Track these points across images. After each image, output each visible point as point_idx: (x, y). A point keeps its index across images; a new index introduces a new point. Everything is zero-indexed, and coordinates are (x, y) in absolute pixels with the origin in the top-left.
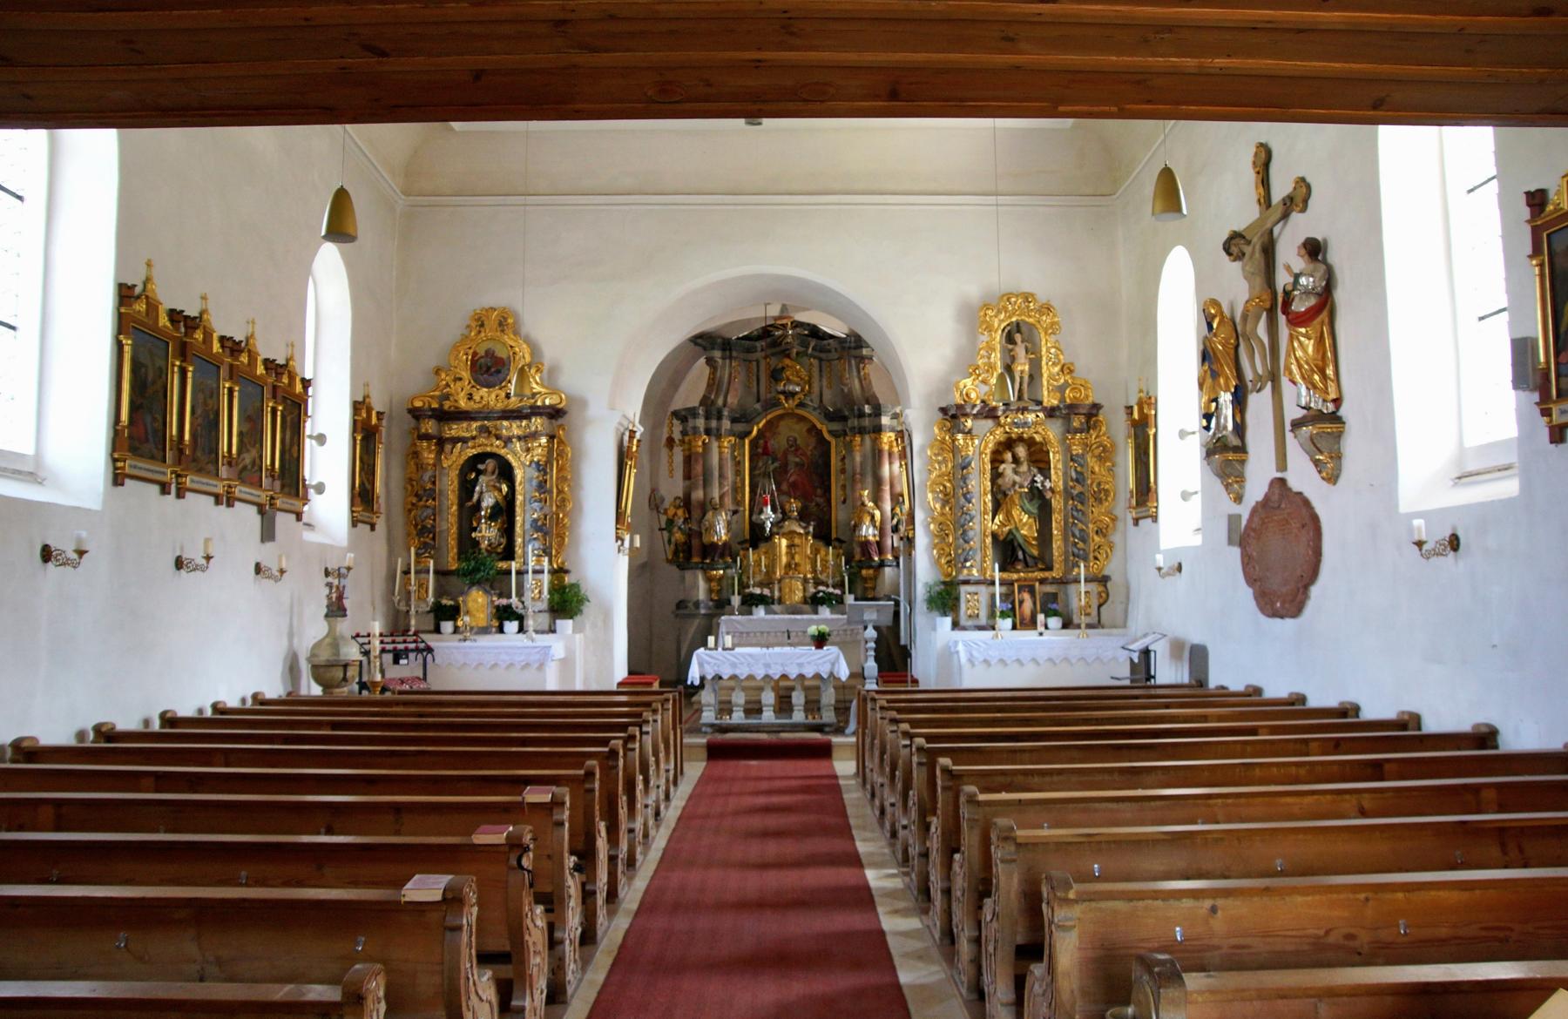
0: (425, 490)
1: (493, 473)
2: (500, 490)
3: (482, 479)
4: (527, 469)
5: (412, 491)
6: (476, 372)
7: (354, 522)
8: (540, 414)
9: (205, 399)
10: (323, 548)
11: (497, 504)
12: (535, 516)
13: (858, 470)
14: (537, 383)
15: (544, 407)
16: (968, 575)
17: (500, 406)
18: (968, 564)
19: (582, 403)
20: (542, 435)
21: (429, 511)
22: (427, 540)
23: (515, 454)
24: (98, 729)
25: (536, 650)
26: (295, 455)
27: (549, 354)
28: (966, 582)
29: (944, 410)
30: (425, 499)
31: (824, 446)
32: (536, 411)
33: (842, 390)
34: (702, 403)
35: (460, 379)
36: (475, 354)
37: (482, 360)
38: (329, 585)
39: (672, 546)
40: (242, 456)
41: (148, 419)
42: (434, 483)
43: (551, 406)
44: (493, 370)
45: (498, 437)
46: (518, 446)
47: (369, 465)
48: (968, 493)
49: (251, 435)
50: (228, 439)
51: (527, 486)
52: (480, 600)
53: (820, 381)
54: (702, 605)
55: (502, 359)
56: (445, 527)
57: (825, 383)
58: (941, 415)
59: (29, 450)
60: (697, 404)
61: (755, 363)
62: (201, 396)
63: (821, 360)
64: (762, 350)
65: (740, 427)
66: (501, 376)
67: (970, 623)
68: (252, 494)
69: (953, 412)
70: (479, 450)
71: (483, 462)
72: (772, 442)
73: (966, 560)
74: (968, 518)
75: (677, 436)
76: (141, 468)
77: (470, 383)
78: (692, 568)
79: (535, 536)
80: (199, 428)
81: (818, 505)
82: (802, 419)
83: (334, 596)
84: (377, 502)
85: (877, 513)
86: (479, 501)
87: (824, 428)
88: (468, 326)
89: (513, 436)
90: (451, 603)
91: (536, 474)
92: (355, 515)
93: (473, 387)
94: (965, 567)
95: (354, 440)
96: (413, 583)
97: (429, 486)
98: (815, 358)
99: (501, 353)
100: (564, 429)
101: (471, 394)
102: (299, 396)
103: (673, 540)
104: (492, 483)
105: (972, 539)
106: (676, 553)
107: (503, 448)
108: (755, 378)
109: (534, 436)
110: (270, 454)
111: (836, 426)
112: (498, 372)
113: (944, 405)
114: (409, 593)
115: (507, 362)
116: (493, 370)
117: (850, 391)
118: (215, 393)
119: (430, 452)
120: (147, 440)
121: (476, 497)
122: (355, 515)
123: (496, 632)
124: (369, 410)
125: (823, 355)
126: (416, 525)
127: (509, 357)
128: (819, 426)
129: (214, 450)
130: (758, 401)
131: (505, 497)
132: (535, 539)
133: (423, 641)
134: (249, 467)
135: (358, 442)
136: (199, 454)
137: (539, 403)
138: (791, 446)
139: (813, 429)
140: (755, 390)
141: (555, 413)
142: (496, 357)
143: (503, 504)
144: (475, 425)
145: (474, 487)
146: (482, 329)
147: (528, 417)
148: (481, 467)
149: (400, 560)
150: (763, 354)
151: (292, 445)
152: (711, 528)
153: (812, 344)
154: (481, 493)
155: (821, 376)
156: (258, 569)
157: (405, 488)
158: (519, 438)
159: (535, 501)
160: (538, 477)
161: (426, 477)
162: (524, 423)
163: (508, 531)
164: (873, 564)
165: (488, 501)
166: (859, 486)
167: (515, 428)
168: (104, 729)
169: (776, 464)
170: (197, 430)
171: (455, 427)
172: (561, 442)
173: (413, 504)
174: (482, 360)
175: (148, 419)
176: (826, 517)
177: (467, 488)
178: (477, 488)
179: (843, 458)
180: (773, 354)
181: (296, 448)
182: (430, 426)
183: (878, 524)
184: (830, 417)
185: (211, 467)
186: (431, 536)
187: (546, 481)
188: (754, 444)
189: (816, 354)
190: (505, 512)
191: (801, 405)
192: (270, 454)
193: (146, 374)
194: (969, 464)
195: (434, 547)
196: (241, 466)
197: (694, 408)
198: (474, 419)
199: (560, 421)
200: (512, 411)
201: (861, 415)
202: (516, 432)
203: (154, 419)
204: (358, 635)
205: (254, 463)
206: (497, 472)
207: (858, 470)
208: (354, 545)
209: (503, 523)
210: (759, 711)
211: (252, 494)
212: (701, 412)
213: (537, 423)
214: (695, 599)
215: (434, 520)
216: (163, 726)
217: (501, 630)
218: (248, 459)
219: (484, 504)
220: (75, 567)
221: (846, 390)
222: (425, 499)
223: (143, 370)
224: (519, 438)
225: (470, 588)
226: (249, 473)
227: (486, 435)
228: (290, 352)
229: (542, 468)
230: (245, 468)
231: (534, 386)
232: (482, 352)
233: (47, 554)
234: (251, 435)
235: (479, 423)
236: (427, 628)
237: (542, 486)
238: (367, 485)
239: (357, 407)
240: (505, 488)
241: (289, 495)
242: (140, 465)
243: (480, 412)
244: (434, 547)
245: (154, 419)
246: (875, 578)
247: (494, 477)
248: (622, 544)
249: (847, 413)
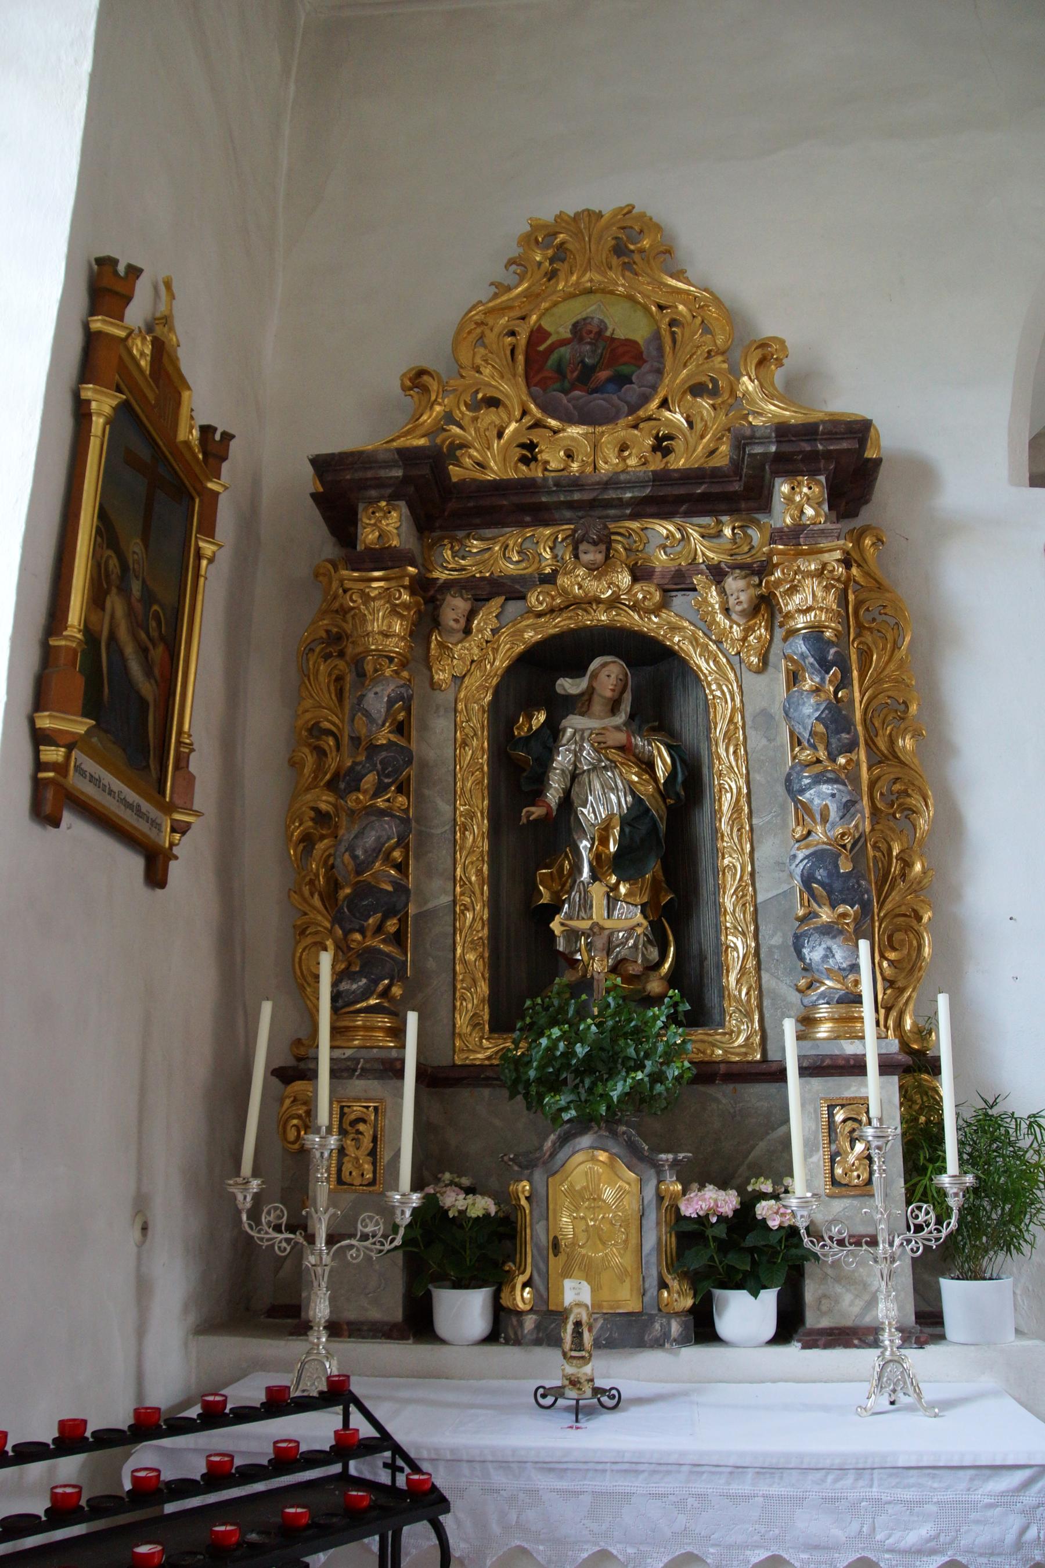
0: (373, 749)
1: (614, 707)
2: (648, 766)
3: (573, 724)
5: (319, 769)
6: (543, 384)
21: (390, 828)
22: (376, 942)
25: (1019, 1477)
30: (369, 780)
35: (493, 402)
37: (565, 351)
42: (401, 729)
44: (604, 375)
52: (608, 1194)
56: (445, 899)
66: (632, 391)
71: (578, 669)
77: (524, 413)
79: (826, 915)
84: (182, 763)
86: (567, 804)
88: (511, 262)
90: (482, 1206)
92: (53, 754)
93: (538, 425)
95: (81, 413)
96: (323, 1116)
97: (384, 736)
101: (531, 446)
104: (621, 738)
112: (622, 380)
114: (302, 1155)
116: (604, 375)
119: (394, 611)
121: (553, 796)
122: (53, 754)
123: (684, 1341)
126: (330, 896)
127: (657, 336)
135: (98, 423)
142: (612, 340)
143: (657, 810)
146: (563, 267)
149: (267, 1009)
154: (574, 776)
157: (295, 764)
161: (377, 701)
171: (476, 545)
173: (321, 818)
174: (565, 351)
186: (392, 925)
195: (398, 974)
202: (705, 551)
206: (626, 707)
209: (655, 889)
215: (401, 868)
222: (369, 780)
224: (717, 574)
225: (565, 1139)
232: (565, 333)
236: (375, 1314)
244: (398, 974)
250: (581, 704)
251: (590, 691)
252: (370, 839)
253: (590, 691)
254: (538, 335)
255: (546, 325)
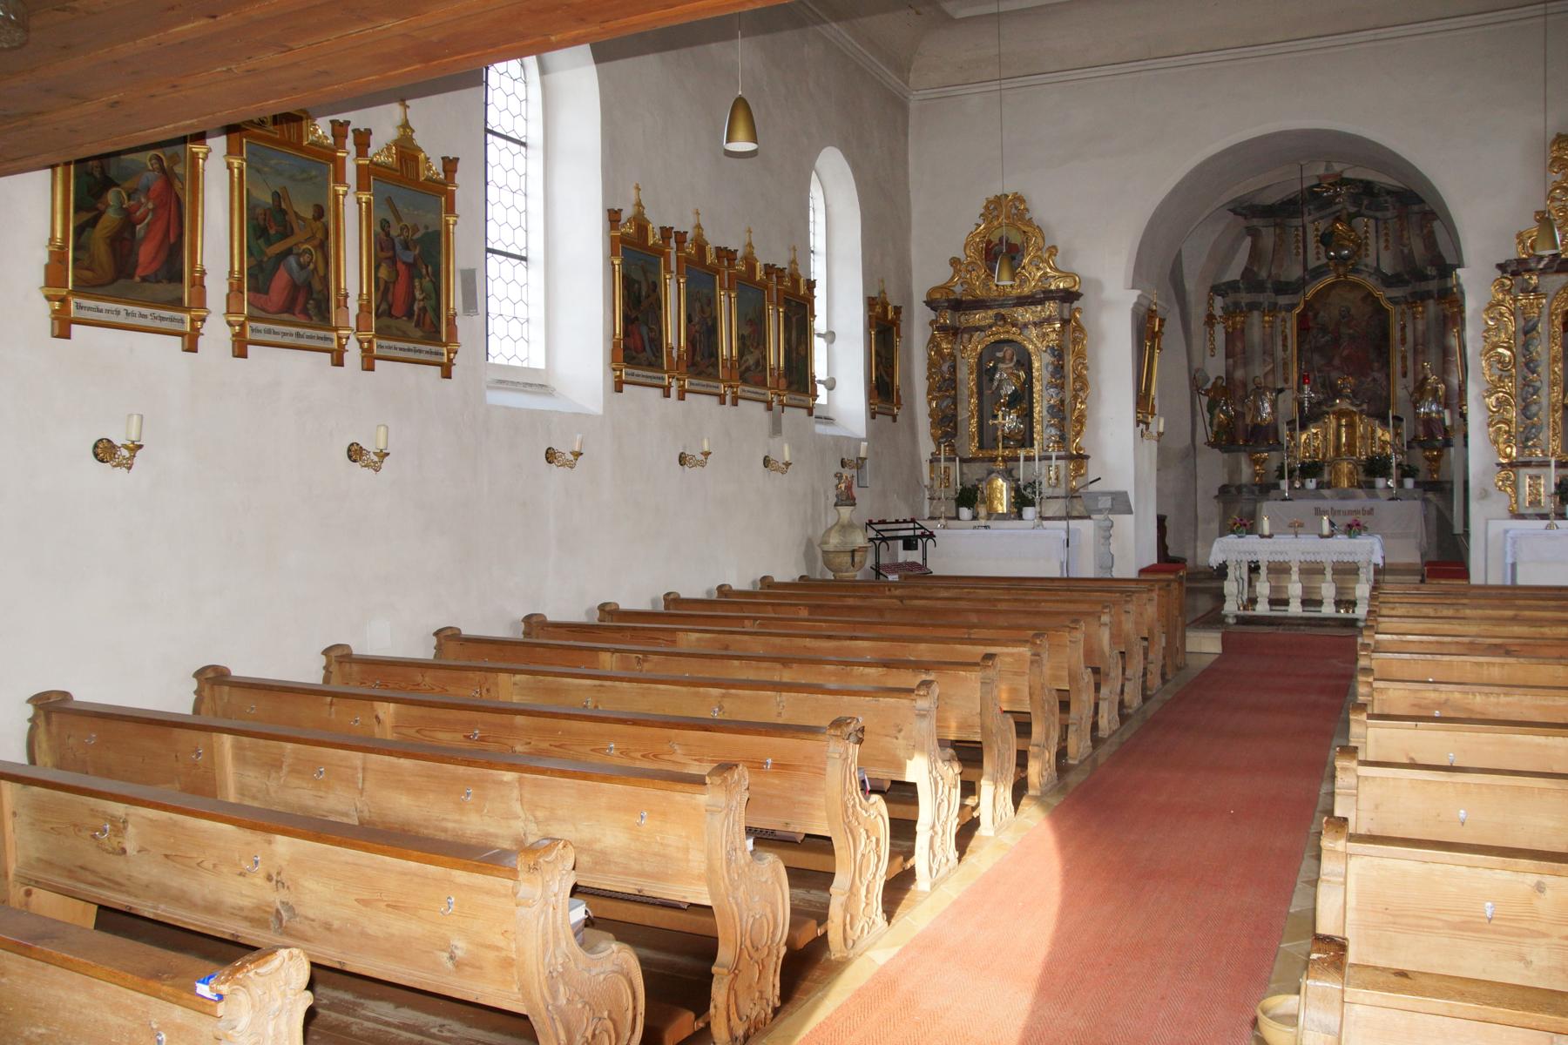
1: (1012, 359)
2: (1018, 377)
4: (1044, 355)
7: (873, 414)
8: (1053, 299)
9: (702, 307)
10: (838, 440)
11: (1015, 391)
12: (1052, 402)
13: (1420, 341)
14: (1051, 268)
15: (1058, 290)
16: (1530, 455)
17: (1016, 292)
18: (1530, 444)
19: (1098, 285)
20: (1056, 319)
23: (1031, 341)
24: (602, 607)
26: (803, 353)
27: (1059, 238)
28: (1527, 464)
29: (1501, 267)
31: (1381, 313)
32: (1049, 295)
33: (1402, 252)
34: (1243, 275)
36: (989, 242)
38: (839, 476)
39: (1215, 429)
40: (744, 358)
41: (644, 330)
43: (1066, 290)
45: (1014, 325)
46: (1034, 332)
47: (887, 359)
48: (1531, 360)
49: (753, 337)
50: (727, 345)
51: (1044, 372)
53: (1377, 242)
54: (1244, 490)
55: (1016, 245)
57: (1382, 244)
58: (1498, 273)
59: (541, 365)
60: (1238, 278)
61: (1301, 229)
62: (697, 306)
63: (1377, 219)
64: (1310, 214)
65: (1283, 300)
67: (1531, 511)
68: (757, 393)
69: (1513, 268)
70: (996, 338)
72: (1322, 313)
73: (1527, 439)
74: (1531, 390)
75: (1218, 312)
76: (638, 376)
78: (1234, 451)
80: (698, 335)
81: (1374, 380)
82: (1356, 286)
83: (843, 486)
85: (1441, 386)
86: (999, 387)
87: (1382, 294)
88: (981, 215)
89: (1029, 323)
91: (1052, 359)
94: (1526, 447)
98: (1369, 217)
99: (1016, 239)
100: (1079, 312)
102: (802, 297)
103: (1216, 421)
105: (1536, 415)
106: (1216, 434)
107: (1020, 334)
108: (1301, 245)
109: (1049, 320)
110: (775, 355)
111: (1396, 293)
113: (1502, 261)
115: (1021, 248)
117: (1411, 251)
118: (711, 302)
120: (644, 349)
121: (996, 384)
124: (885, 306)
125: (1379, 214)
128: (1378, 294)
129: (713, 352)
130: (1305, 268)
131: (1024, 383)
132: (1052, 425)
133: (922, 528)
134: (753, 367)
136: (698, 358)
137: (1053, 287)
138: (1343, 318)
139: (1369, 297)
140: (1301, 257)
141: (1069, 296)
144: (991, 313)
145: (994, 375)
147: (1041, 302)
148: (999, 355)
150: (1311, 218)
151: (799, 343)
152: (1258, 410)
153: (1365, 202)
154: (1000, 381)
155: (1377, 237)
156: (767, 462)
158: (1035, 324)
159: (1051, 387)
160: (1053, 363)
162: (1039, 308)
163: (1027, 416)
164: (1437, 444)
165: (1009, 389)
166: (1421, 357)
167: (1026, 315)
168: (607, 608)
169: (1327, 338)
170: (694, 337)
172: (1079, 328)
175: (644, 330)
176: (1384, 394)
177: (985, 374)
178: (997, 376)
179: (1403, 328)
180: (1321, 218)
181: (804, 347)
182: (947, 319)
183: (1442, 400)
184: (1389, 281)
185: (711, 370)
187: (1062, 367)
188: (1302, 318)
189: (1371, 213)
190: (1021, 400)
191: (1356, 271)
192: (775, 355)
193: (640, 289)
194: (1534, 328)
196: (743, 368)
197: (1235, 282)
198: (989, 308)
199: (1076, 304)
200: (1027, 297)
201: (1424, 278)
203: (651, 330)
204: (870, 523)
205: (757, 363)
207: (1420, 341)
208: (873, 434)
210: (1286, 603)
211: (757, 393)
212: (1241, 285)
213: (1051, 308)
214: (1238, 483)
216: (666, 607)
217: (1020, 517)
218: (750, 360)
219: (1003, 392)
220: (571, 468)
221: (1406, 251)
223: (636, 286)
224: (1035, 324)
226: (750, 373)
227: (1000, 323)
228: (792, 256)
229: (1058, 353)
230: (748, 369)
231: (1048, 270)
232: (997, 242)
233: (550, 456)
234: (753, 337)
235: (995, 311)
237: (1058, 370)
238: (885, 377)
239: (870, 303)
240: (1022, 374)
241: (798, 391)
242: (636, 372)
243: (995, 300)
245: (651, 330)
246: (1440, 456)
247: (1012, 365)
248: (1147, 428)
249: (1406, 277)
250: (1003, 360)
251: (1004, 356)
252: (945, 404)
253: (1004, 356)
254: (989, 242)
255: (992, 238)
